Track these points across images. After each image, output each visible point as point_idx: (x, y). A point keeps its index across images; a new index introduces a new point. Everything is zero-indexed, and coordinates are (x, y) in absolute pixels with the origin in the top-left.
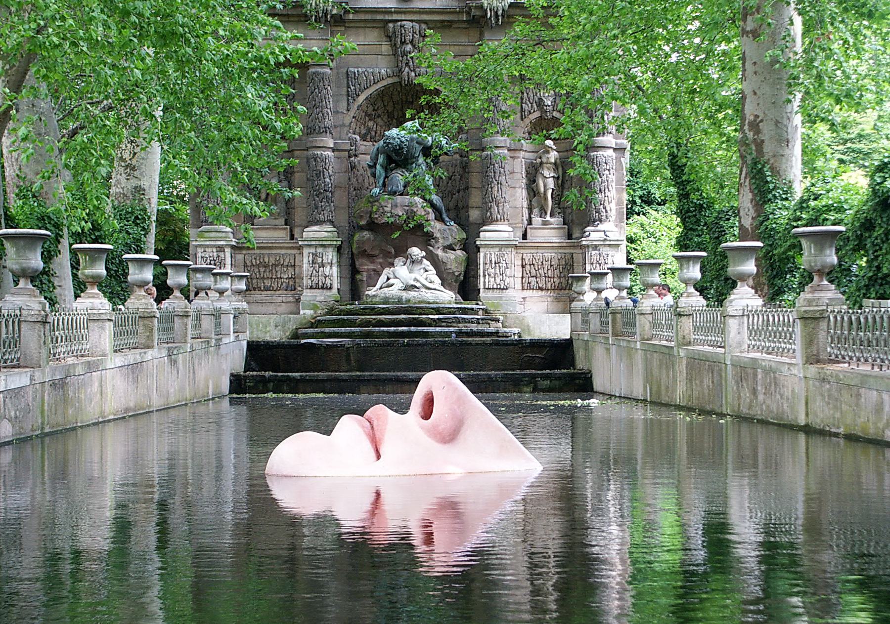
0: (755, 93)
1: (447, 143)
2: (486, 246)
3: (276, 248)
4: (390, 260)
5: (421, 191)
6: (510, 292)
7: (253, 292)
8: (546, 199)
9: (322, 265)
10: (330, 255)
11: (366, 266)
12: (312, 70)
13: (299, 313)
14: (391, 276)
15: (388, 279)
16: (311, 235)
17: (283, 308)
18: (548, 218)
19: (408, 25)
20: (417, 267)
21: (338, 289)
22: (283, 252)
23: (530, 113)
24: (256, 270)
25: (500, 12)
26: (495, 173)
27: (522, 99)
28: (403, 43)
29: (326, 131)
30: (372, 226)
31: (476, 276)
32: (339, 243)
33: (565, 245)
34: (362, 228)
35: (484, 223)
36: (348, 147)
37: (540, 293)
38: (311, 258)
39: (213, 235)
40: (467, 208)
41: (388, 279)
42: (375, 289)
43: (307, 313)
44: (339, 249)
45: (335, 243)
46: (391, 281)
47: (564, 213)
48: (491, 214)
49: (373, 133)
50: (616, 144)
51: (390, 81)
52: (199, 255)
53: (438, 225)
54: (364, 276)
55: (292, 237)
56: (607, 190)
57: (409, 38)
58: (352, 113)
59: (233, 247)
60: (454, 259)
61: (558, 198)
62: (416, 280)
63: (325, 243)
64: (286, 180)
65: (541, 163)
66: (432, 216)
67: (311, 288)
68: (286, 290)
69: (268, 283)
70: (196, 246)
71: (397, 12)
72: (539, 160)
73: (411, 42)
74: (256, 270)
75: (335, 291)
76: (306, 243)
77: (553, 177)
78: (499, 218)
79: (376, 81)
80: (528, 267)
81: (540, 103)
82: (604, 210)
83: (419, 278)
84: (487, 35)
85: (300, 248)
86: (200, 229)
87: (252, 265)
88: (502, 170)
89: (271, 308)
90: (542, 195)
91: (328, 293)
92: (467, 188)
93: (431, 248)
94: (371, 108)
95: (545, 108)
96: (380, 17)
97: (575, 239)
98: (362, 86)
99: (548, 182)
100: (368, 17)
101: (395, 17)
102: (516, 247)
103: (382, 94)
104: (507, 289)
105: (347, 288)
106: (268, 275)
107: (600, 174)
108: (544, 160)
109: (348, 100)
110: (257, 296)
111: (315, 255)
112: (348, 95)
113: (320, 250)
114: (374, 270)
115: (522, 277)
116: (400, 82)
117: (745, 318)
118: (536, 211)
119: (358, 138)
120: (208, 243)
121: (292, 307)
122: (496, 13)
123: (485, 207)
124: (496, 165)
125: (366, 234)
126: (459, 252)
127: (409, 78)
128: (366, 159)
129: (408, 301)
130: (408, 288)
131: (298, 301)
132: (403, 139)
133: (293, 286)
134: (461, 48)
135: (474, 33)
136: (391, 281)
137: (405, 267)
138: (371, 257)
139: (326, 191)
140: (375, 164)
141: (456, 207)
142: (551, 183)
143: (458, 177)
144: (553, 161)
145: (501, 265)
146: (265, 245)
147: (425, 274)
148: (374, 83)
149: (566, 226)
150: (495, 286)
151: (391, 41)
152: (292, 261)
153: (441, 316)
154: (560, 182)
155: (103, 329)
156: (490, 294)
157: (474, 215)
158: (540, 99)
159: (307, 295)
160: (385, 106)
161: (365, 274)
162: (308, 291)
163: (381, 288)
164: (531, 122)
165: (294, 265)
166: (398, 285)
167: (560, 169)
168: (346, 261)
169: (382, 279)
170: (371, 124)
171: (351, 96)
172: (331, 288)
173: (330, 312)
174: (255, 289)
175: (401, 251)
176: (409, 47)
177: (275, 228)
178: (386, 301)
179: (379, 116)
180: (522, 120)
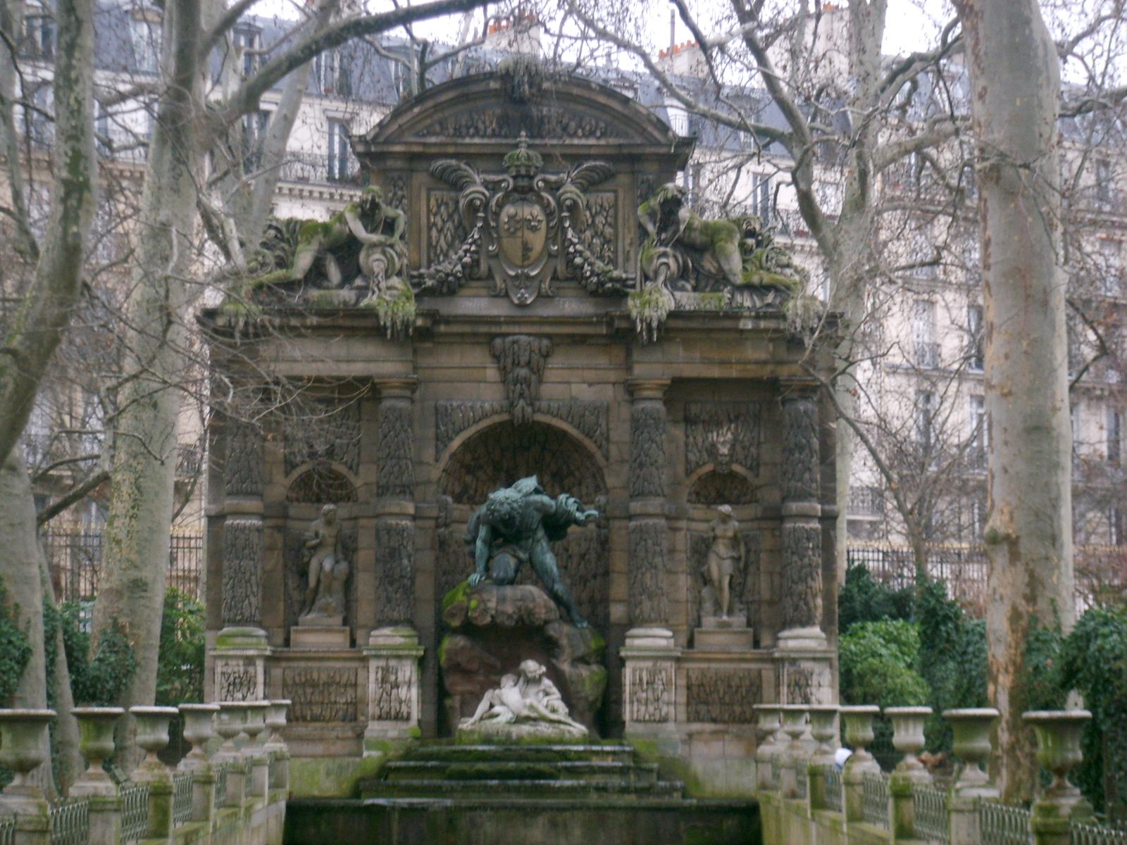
0: (1006, 471)
1: (578, 510)
2: (634, 658)
3: (329, 659)
4: (494, 678)
5: (538, 575)
6: (671, 726)
7: (294, 723)
8: (721, 589)
9: (396, 685)
10: (408, 671)
11: (459, 686)
12: (387, 404)
13: (360, 755)
14: (496, 702)
15: (492, 706)
16: (381, 641)
17: (338, 748)
18: (725, 618)
19: (523, 338)
20: (533, 690)
21: (419, 721)
22: (338, 665)
24: (300, 692)
25: (655, 324)
27: (687, 445)
28: (516, 364)
29: (406, 490)
30: (469, 629)
31: (619, 702)
32: (422, 653)
33: (749, 656)
34: (455, 631)
35: (631, 623)
36: (434, 513)
37: (709, 727)
38: (380, 675)
39: (239, 640)
40: (606, 601)
41: (492, 706)
42: (472, 720)
43: (372, 755)
44: (421, 662)
45: (414, 653)
46: (497, 709)
47: (748, 609)
48: (642, 612)
49: (472, 492)
50: (823, 511)
51: (497, 419)
52: (219, 670)
53: (566, 628)
54: (454, 702)
55: (353, 643)
57: (524, 359)
58: (442, 465)
59: (268, 659)
60: (588, 677)
61: (739, 587)
62: (531, 707)
63: (401, 653)
64: (346, 559)
65: (715, 538)
66: (555, 614)
67: (380, 718)
68: (343, 720)
69: (317, 710)
70: (215, 657)
71: (511, 321)
72: (711, 534)
74: (300, 692)
75: (414, 722)
76: (373, 653)
77: (732, 558)
80: (695, 690)
81: (712, 451)
82: (805, 608)
83: (535, 703)
84: (636, 356)
85: (364, 660)
86: (220, 633)
87: (295, 684)
89: (319, 749)
90: (716, 584)
91: (403, 726)
92: (606, 573)
93: (554, 661)
94: (468, 457)
96: (483, 329)
97: (765, 648)
99: (721, 565)
100: (467, 329)
101: (505, 329)
102: (678, 660)
103: (485, 437)
105: (431, 716)
106: (317, 698)
108: (719, 532)
109: (437, 446)
110: (301, 729)
111: (386, 671)
112: (437, 439)
113: (392, 663)
114: (471, 693)
115: (688, 704)
116: (511, 422)
117: (977, 815)
118: (708, 606)
119: (450, 499)
120: (231, 653)
121: (350, 746)
122: (649, 325)
123: (631, 602)
124: (650, 542)
125: (461, 641)
126: (595, 667)
128: (462, 531)
129: (520, 740)
130: (519, 720)
131: (360, 736)
132: (515, 505)
133: (353, 715)
134: (600, 372)
135: (618, 354)
136: (497, 709)
137: (516, 689)
138: (466, 673)
139: (402, 577)
140: (474, 541)
141: (591, 600)
142: (728, 566)
143: (592, 556)
144: (730, 534)
146: (312, 655)
147: (548, 700)
148: (476, 422)
149: (751, 630)
152: (353, 678)
153: (568, 764)
154: (742, 565)
155: (108, 823)
156: (640, 728)
157: (617, 612)
158: (713, 445)
159: (374, 729)
161: (457, 698)
162: (376, 723)
163: (481, 719)
164: (699, 478)
165: (355, 685)
166: (504, 715)
167: (742, 549)
168: (431, 677)
169: (482, 708)
170: (468, 479)
171: (441, 441)
172: (408, 718)
173: (407, 756)
174: (297, 719)
175: (510, 665)
176: (523, 372)
177: (328, 630)
178: (487, 740)
179: (481, 467)
180: (688, 473)
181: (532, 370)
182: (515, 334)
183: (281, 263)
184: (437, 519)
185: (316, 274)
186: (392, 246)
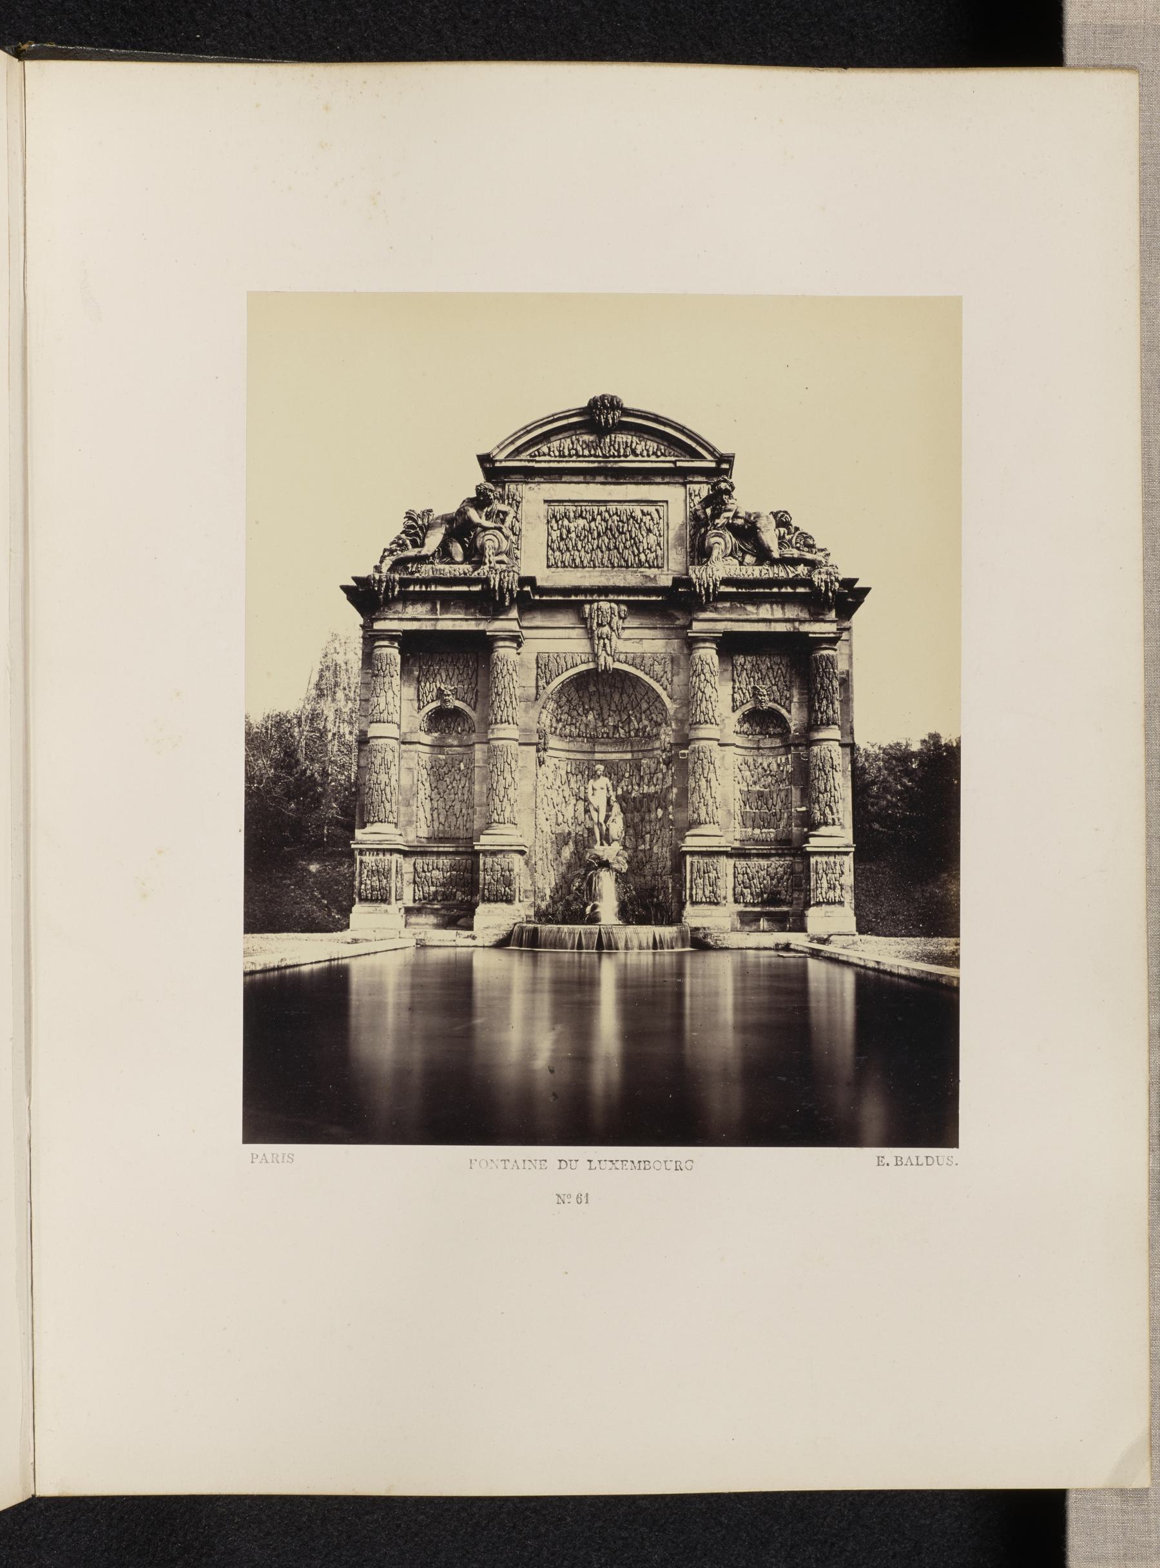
19: (605, 606)
23: (743, 704)
26: (703, 769)
51: (583, 668)
56: (833, 789)
73: (609, 624)
78: (708, 820)
79: (569, 666)
88: (712, 766)
95: (760, 698)
98: (553, 672)
104: (717, 904)
107: (824, 771)
116: (596, 669)
122: (707, 590)
124: (705, 760)
127: (606, 663)
145: (710, 875)
148: (567, 670)
150: (704, 900)
151: (586, 624)
160: (579, 697)
164: (743, 714)
181: (611, 628)
182: (598, 601)
183: (415, 544)
184: (537, 744)
185: (444, 552)
186: (500, 529)
